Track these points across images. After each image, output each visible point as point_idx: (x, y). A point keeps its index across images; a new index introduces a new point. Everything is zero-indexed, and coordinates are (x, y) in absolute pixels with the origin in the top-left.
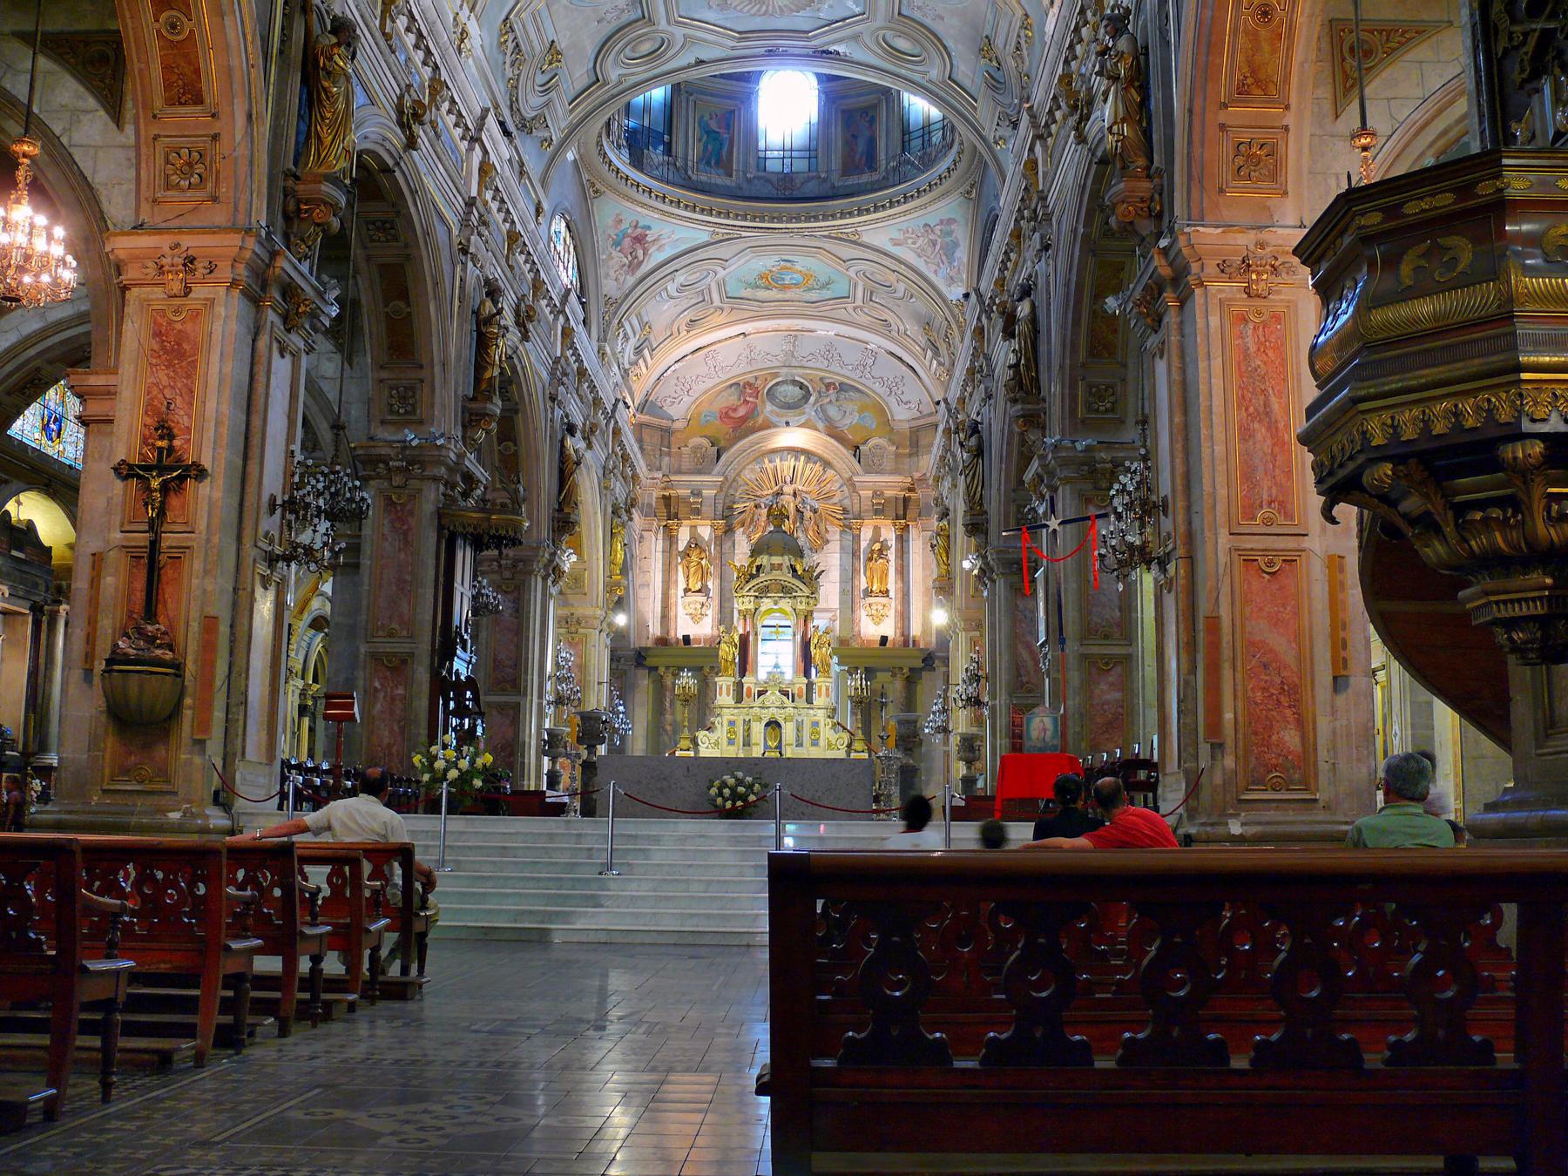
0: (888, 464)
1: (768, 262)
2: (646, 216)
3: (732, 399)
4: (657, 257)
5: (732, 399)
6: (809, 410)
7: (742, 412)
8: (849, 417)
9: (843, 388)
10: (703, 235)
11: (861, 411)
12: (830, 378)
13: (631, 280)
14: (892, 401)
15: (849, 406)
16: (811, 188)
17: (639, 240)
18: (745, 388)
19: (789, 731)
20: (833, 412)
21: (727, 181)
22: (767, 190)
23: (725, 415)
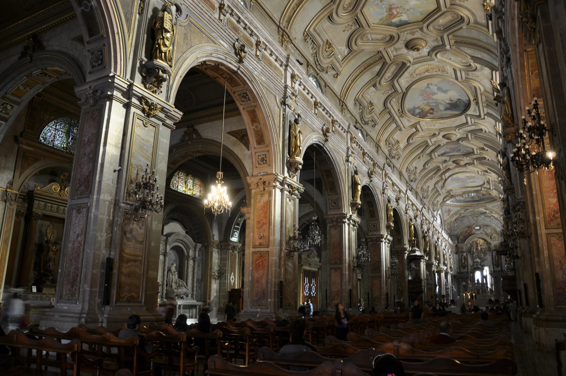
0: (497, 239)
1: (472, 210)
2: (449, 207)
3: (467, 229)
4: (452, 213)
5: (467, 229)
6: (481, 230)
7: (469, 231)
8: (489, 231)
9: (487, 226)
10: (459, 208)
11: (491, 229)
12: (485, 224)
13: (448, 217)
14: (497, 228)
15: (489, 229)
16: (477, 199)
17: (449, 211)
18: (470, 227)
19: (481, 290)
20: (486, 230)
21: (463, 199)
22: (470, 199)
23: (466, 232)
